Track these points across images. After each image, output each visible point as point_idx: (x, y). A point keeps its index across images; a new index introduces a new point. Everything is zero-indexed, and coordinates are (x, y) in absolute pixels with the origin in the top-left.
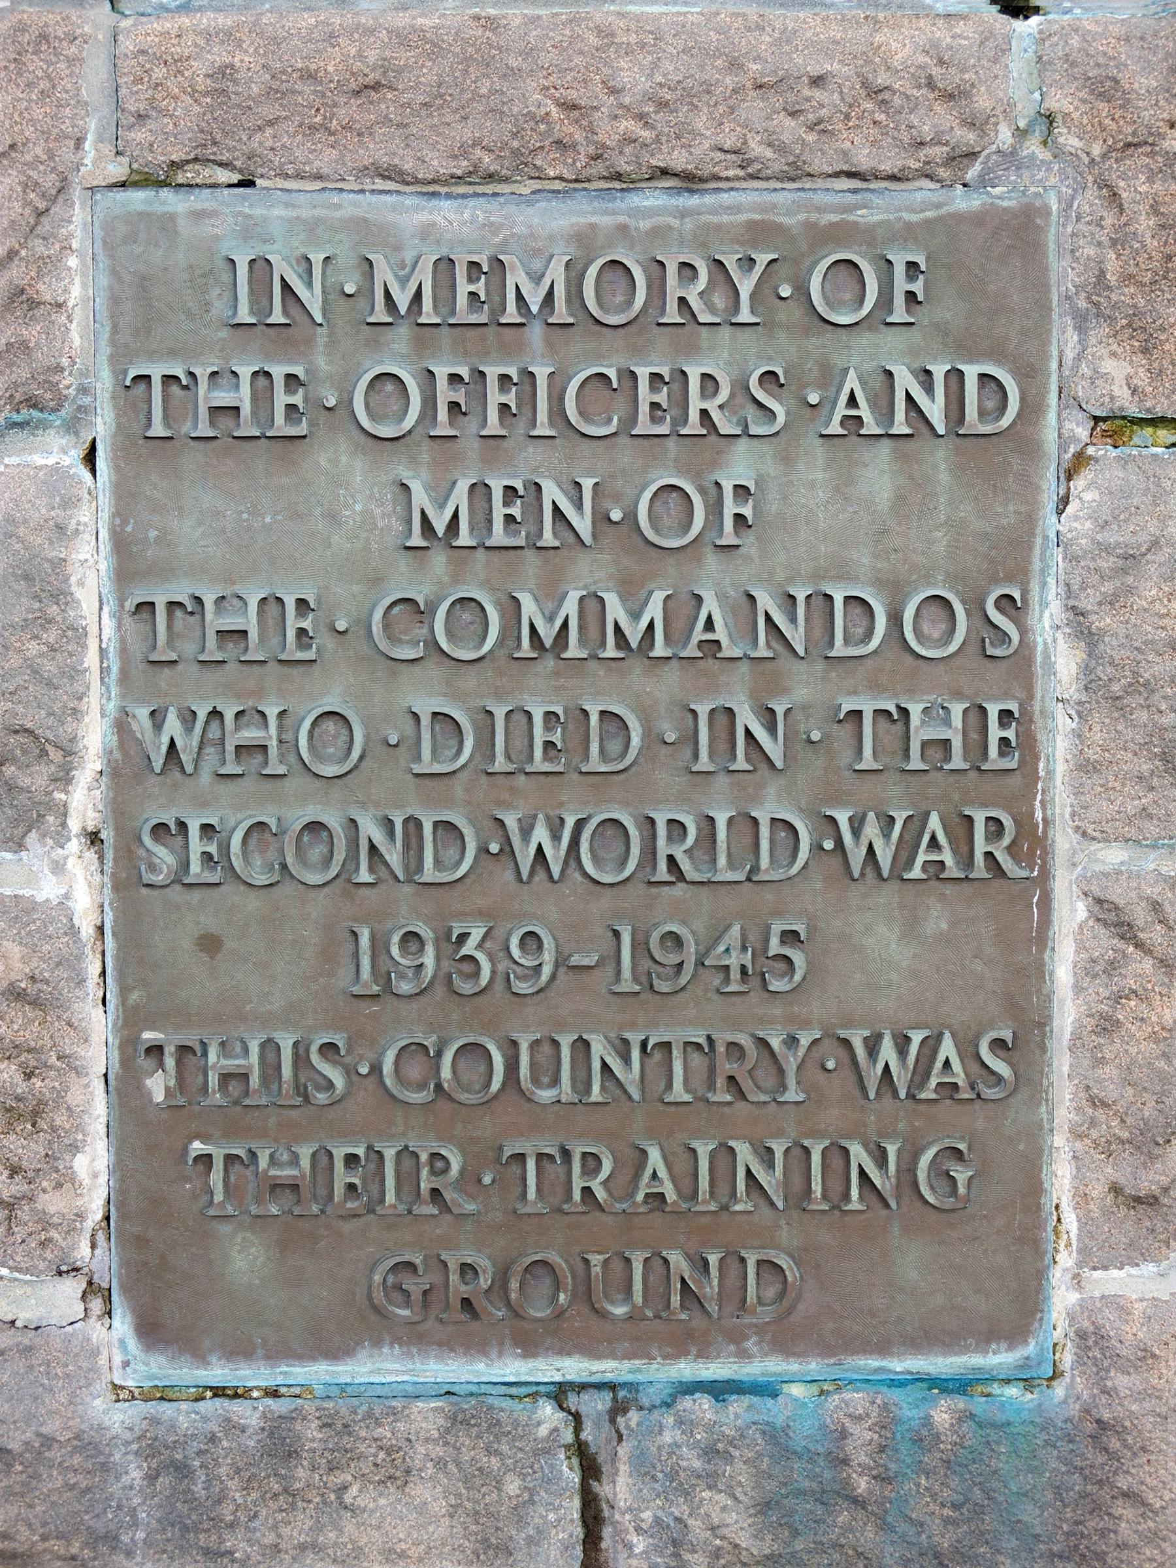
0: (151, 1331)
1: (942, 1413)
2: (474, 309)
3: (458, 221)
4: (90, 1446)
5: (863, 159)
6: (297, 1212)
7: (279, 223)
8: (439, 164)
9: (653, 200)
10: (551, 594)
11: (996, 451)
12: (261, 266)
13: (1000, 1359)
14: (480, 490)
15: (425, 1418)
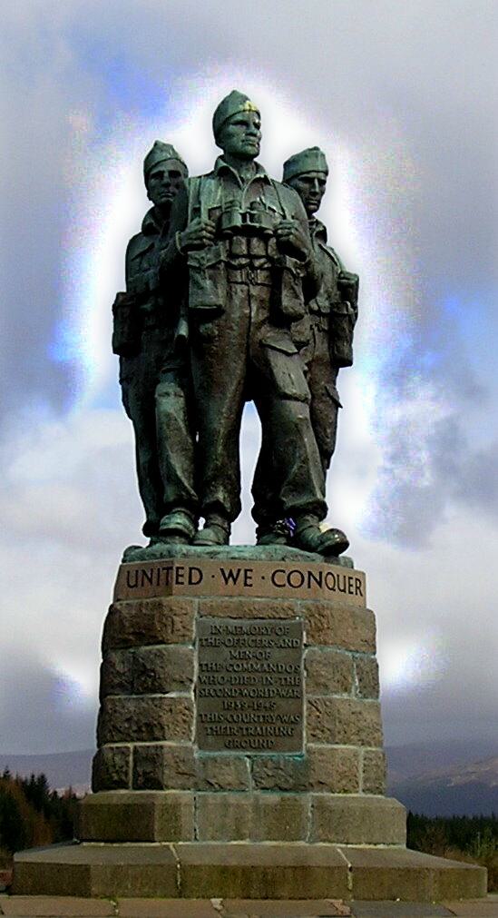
0: (200, 748)
1: (291, 759)
2: (239, 631)
3: (237, 622)
4: (194, 760)
5: (282, 616)
6: (216, 734)
7: (217, 622)
8: (235, 616)
9: (258, 621)
10: (247, 664)
11: (296, 648)
12: (215, 627)
13: (298, 753)
14: (239, 653)
15: (232, 758)
